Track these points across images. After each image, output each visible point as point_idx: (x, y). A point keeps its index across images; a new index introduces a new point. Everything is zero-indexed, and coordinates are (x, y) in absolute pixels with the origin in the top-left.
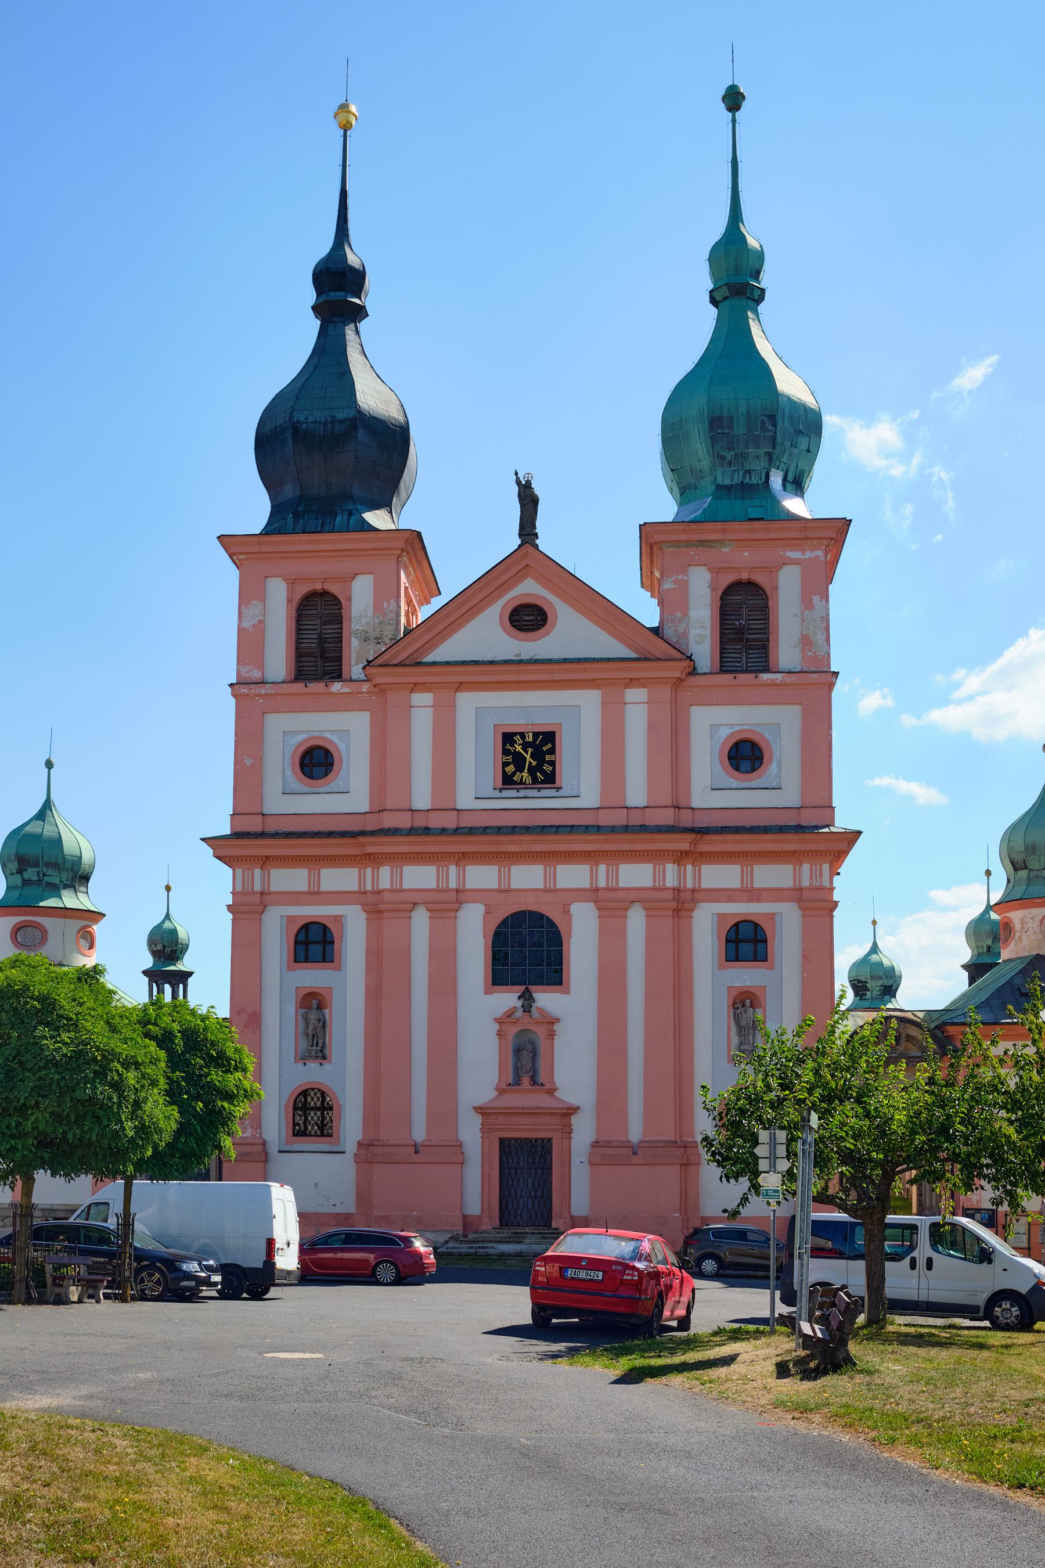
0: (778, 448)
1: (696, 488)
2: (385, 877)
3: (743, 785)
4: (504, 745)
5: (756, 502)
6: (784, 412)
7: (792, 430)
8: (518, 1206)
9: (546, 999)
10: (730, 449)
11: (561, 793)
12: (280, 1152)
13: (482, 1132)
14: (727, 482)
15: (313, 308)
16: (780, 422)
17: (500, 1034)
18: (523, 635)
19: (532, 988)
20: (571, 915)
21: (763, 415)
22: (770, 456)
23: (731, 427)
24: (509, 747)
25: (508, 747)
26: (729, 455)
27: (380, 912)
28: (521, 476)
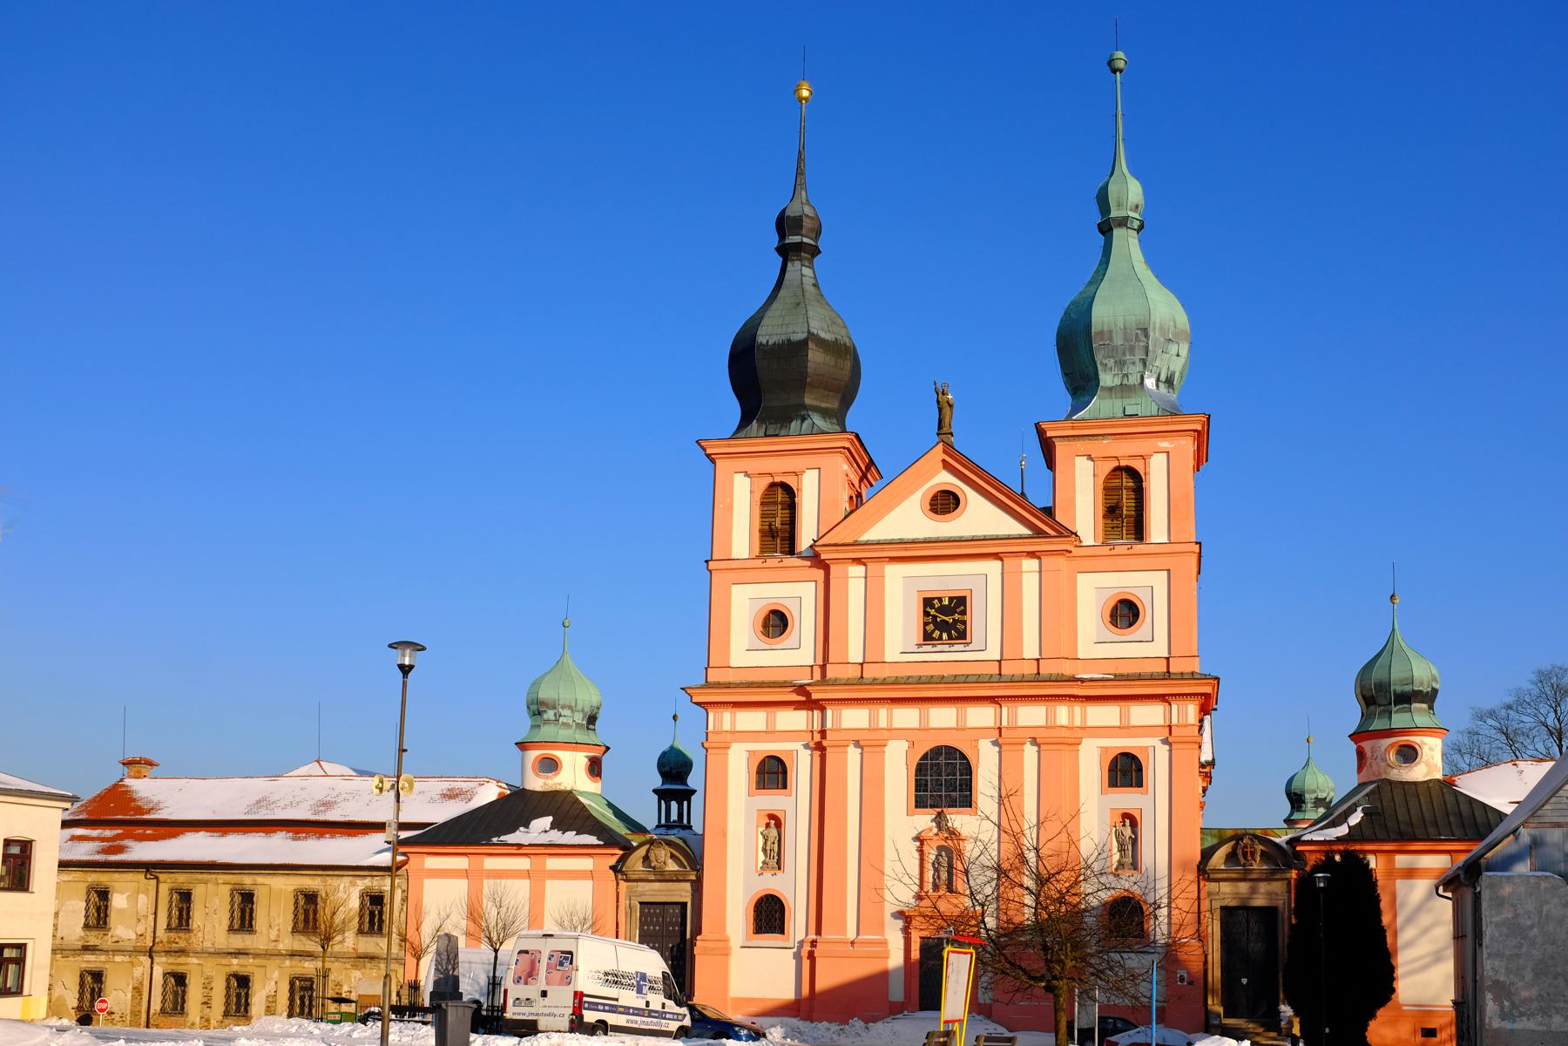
0: (1150, 354)
1: (1084, 389)
3: (1124, 638)
4: (925, 607)
5: (1133, 401)
6: (1155, 323)
7: (1162, 340)
12: (742, 947)
15: (776, 249)
16: (1151, 334)
19: (945, 809)
21: (1138, 329)
22: (1144, 362)
23: (1111, 339)
25: (928, 609)
28: (939, 386)
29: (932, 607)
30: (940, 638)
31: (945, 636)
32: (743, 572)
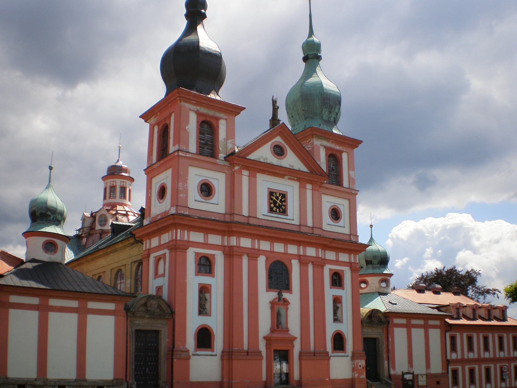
2: (233, 241)
4: (270, 196)
9: (285, 295)
15: (206, 17)
29: (273, 196)
31: (278, 210)
32: (193, 161)
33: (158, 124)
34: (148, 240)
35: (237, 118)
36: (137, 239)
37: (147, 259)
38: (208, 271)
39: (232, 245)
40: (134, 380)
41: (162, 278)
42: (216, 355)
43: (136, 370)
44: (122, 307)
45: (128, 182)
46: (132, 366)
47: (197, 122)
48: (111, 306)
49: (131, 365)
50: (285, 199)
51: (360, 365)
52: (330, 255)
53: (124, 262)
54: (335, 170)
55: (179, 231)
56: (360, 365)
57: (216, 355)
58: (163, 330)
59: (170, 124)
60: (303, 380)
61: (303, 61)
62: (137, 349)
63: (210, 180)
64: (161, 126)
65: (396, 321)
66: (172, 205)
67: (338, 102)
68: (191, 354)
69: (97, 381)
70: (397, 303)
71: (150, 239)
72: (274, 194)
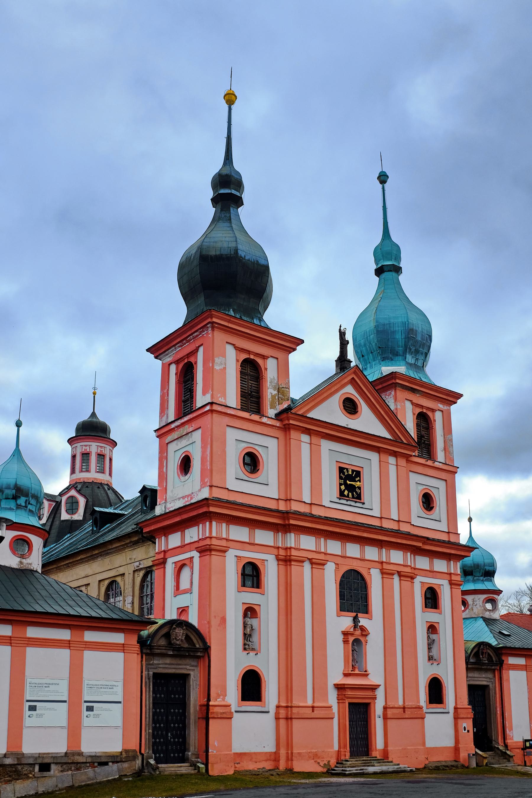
2: (291, 540)
8: (354, 744)
10: (414, 346)
11: (364, 506)
13: (338, 699)
14: (410, 361)
17: (345, 642)
18: (348, 415)
19: (359, 615)
20: (371, 575)
21: (427, 335)
24: (343, 476)
26: (413, 349)
27: (290, 561)
28: (342, 329)
30: (348, 496)
33: (177, 362)
34: (163, 538)
35: (292, 356)
36: (145, 535)
37: (163, 566)
38: (255, 585)
39: (289, 546)
40: (151, 752)
41: (188, 595)
42: (268, 712)
43: (154, 736)
44: (133, 640)
45: (108, 447)
46: (149, 730)
47: (237, 361)
48: (118, 638)
49: (147, 728)
50: (360, 478)
51: (465, 727)
52: (422, 562)
53: (121, 570)
54: (426, 437)
55: (214, 523)
56: (465, 727)
57: (268, 712)
58: (192, 673)
59: (196, 363)
60: (389, 748)
61: (375, 275)
62: (156, 704)
63: (257, 447)
64: (181, 365)
65: (512, 660)
66: (203, 485)
67: (428, 336)
68: (233, 710)
69: (98, 755)
70: (511, 635)
71: (166, 535)
72: (345, 471)
